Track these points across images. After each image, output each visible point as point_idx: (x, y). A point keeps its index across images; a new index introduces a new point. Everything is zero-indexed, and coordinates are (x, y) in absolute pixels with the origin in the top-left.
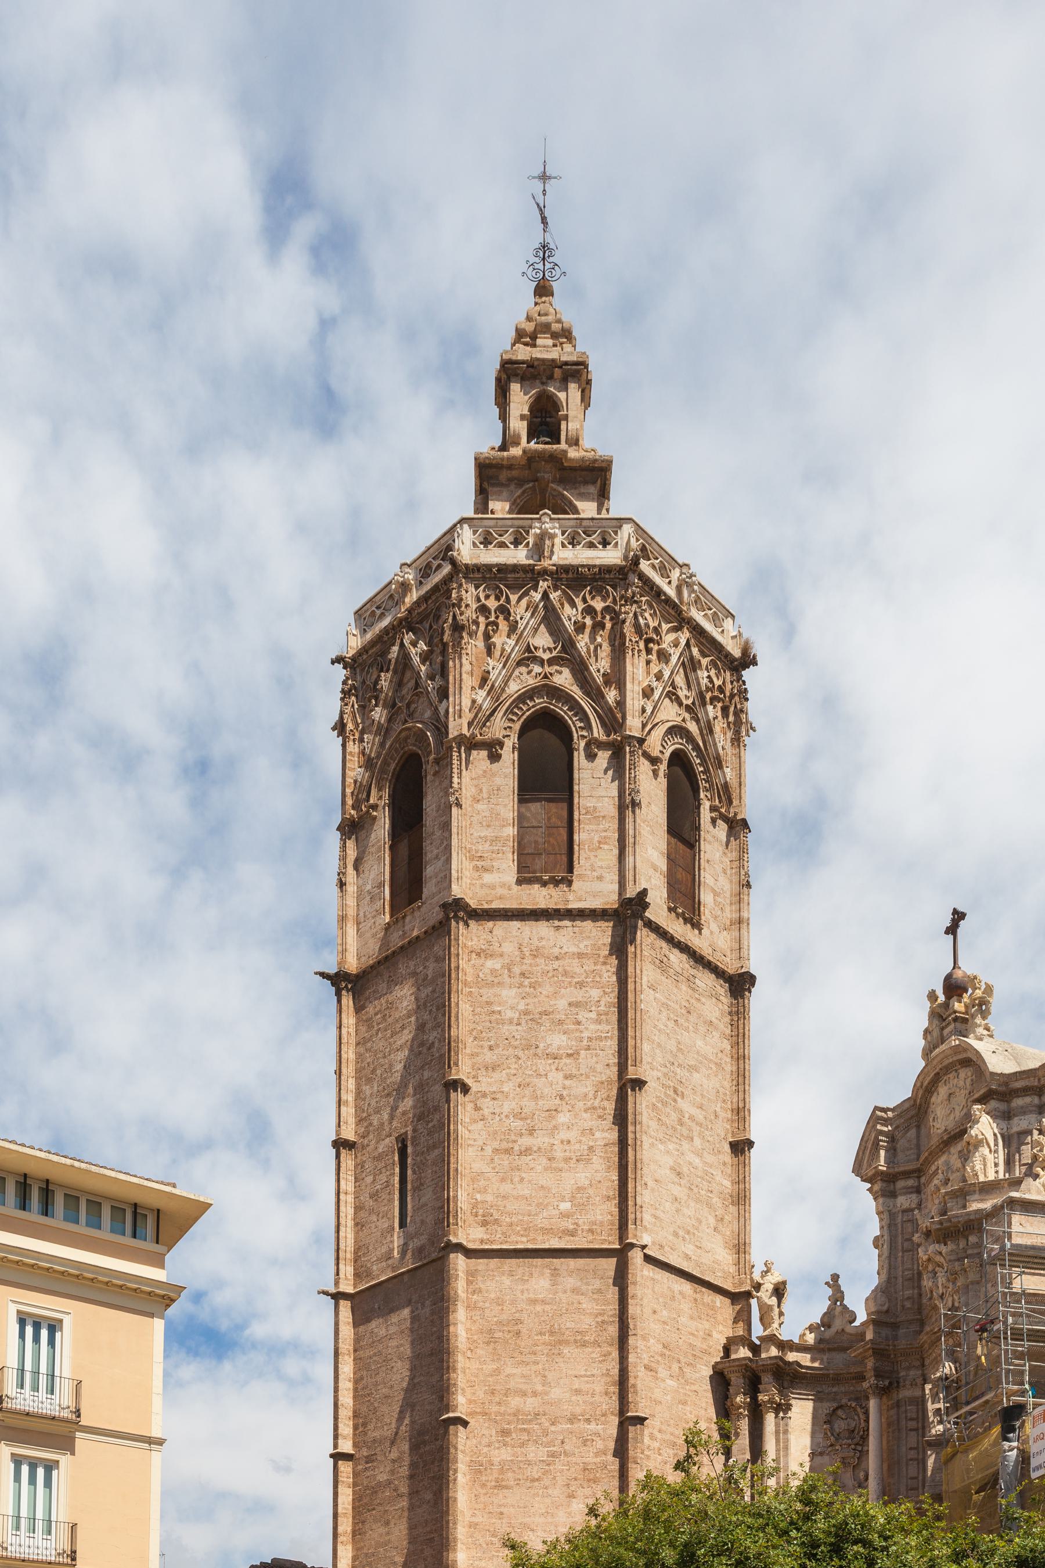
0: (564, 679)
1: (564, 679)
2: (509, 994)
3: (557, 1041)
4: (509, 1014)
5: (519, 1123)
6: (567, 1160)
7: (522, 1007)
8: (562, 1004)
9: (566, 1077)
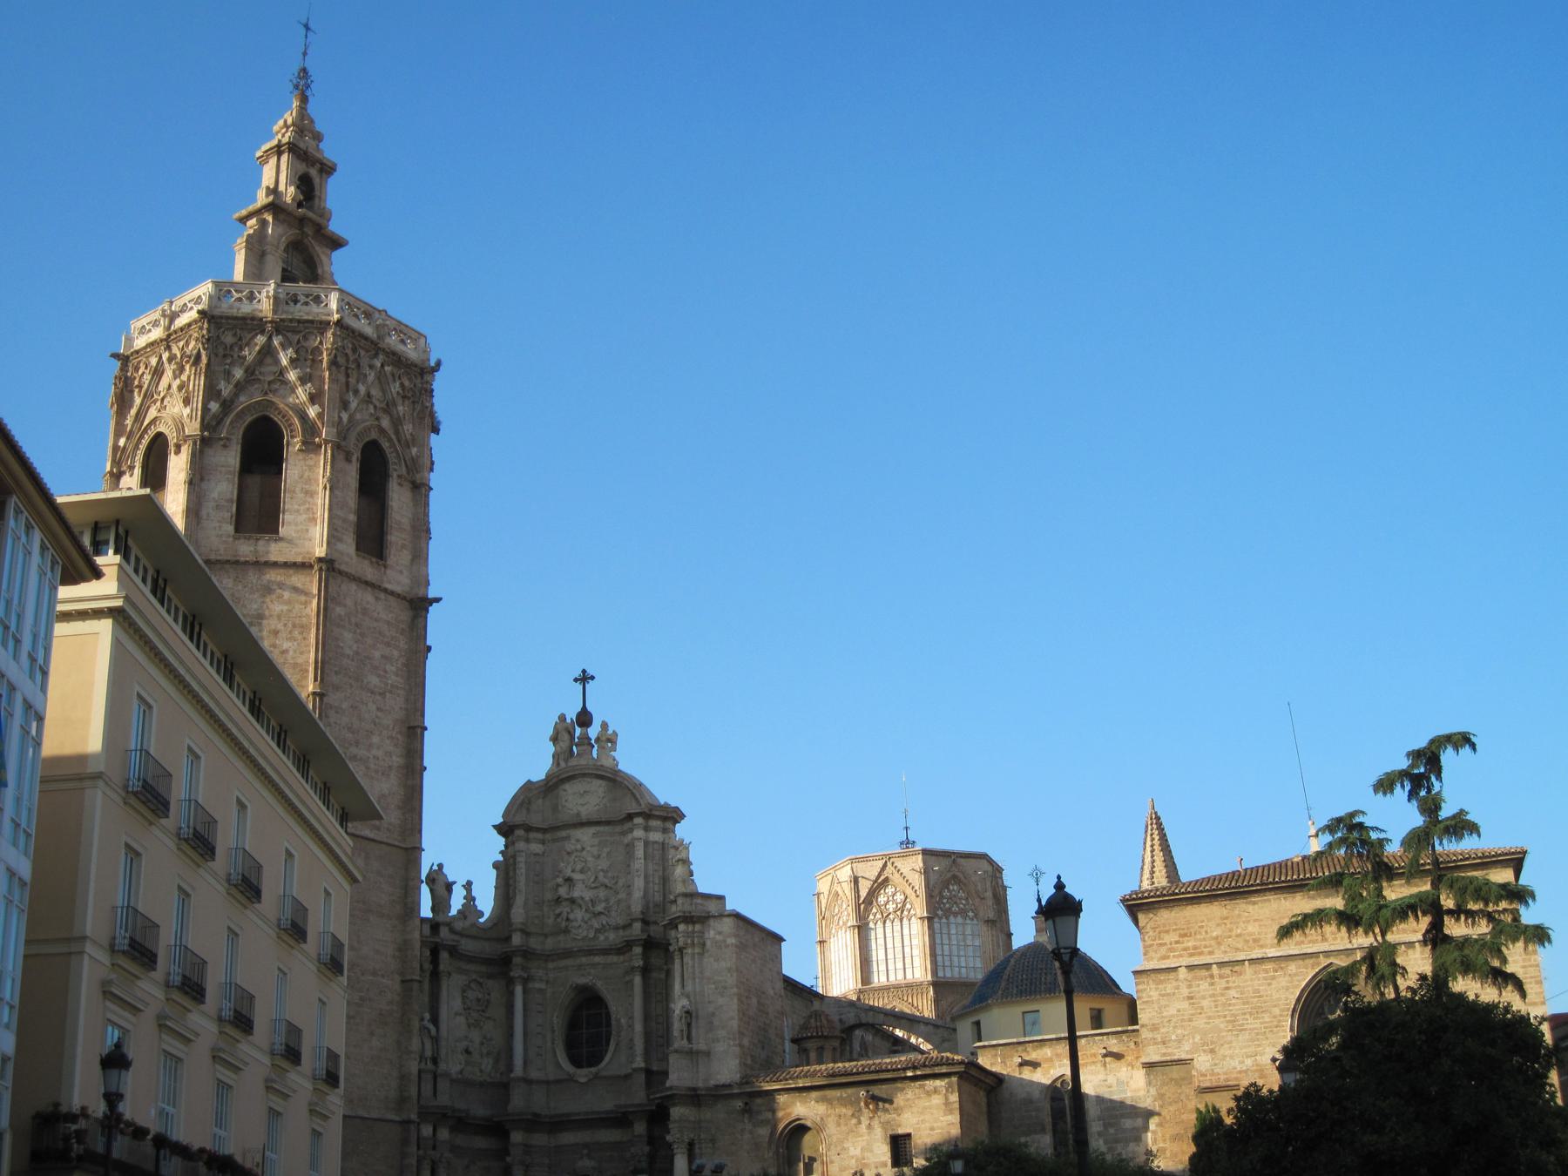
0: (385, 423)
1: (385, 423)
2: (348, 636)
3: (374, 680)
4: (348, 652)
5: (349, 736)
6: (377, 772)
7: (355, 647)
8: (377, 654)
9: (379, 709)
